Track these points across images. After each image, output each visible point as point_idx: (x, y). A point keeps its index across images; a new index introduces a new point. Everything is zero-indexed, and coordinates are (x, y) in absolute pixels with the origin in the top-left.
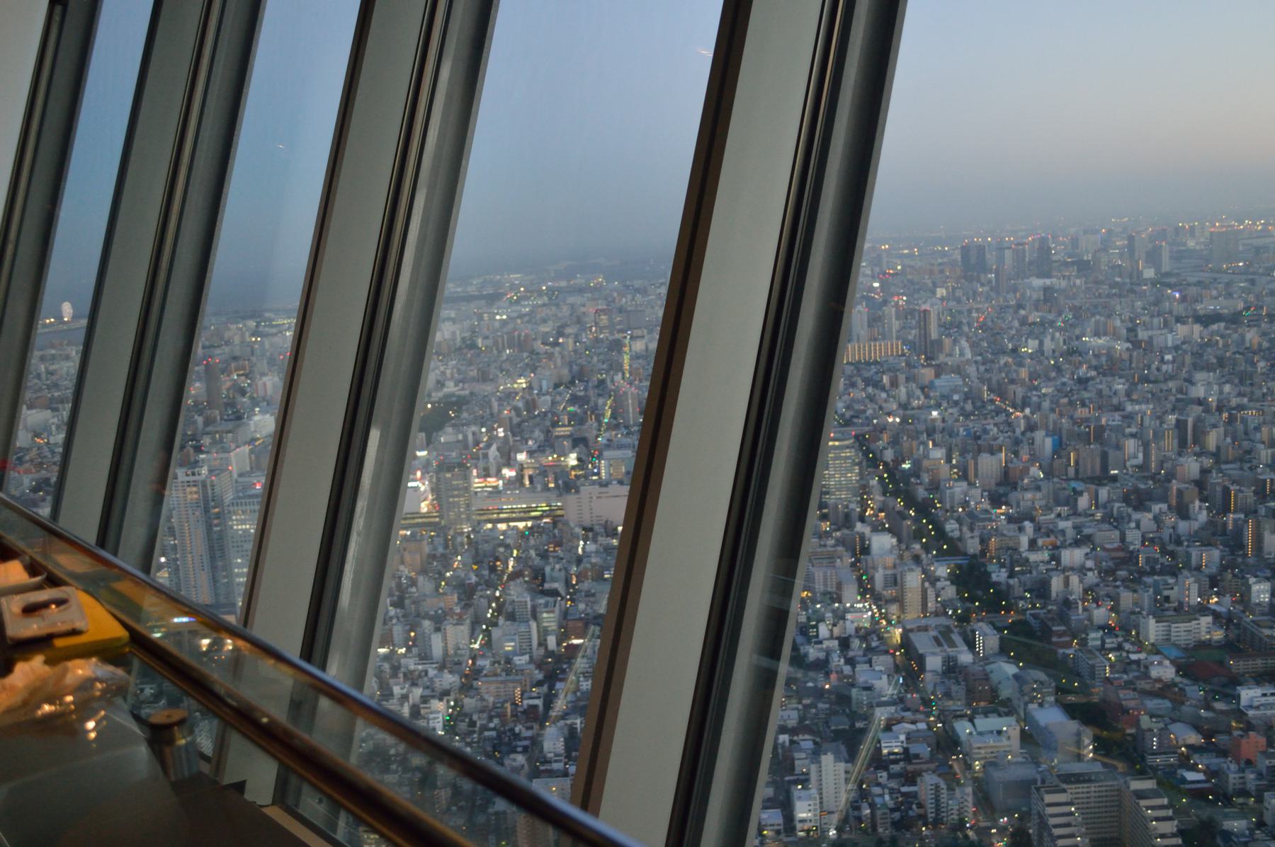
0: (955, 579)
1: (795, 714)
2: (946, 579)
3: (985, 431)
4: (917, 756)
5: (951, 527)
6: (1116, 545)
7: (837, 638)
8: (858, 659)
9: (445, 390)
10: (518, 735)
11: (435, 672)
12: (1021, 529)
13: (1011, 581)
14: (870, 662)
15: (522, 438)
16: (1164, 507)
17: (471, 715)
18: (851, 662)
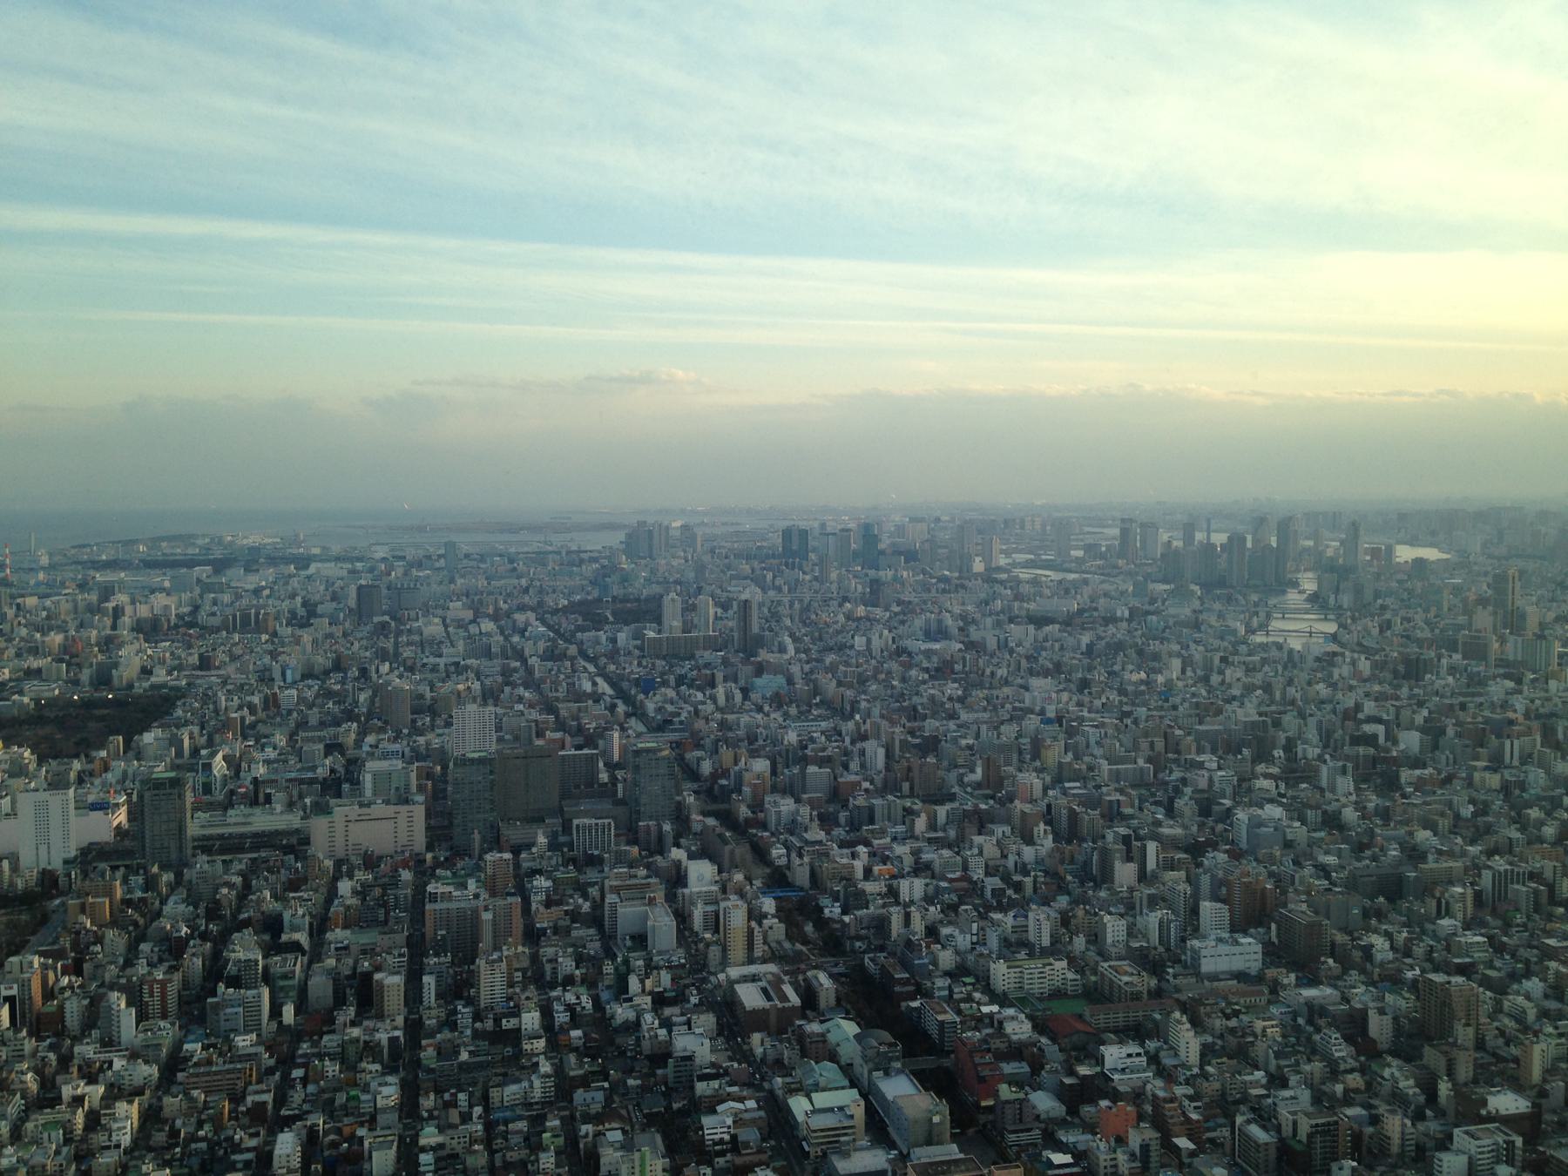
0: (783, 913)
1: (600, 1096)
2: (773, 916)
3: (812, 740)
4: (746, 1145)
5: (778, 852)
6: (958, 874)
7: (651, 993)
8: (675, 1019)
9: (153, 679)
10: (239, 1145)
11: (124, 1063)
12: (854, 856)
13: (847, 919)
14: (688, 1023)
15: (257, 741)
16: (1007, 829)
17: (174, 1122)
18: (667, 1024)
